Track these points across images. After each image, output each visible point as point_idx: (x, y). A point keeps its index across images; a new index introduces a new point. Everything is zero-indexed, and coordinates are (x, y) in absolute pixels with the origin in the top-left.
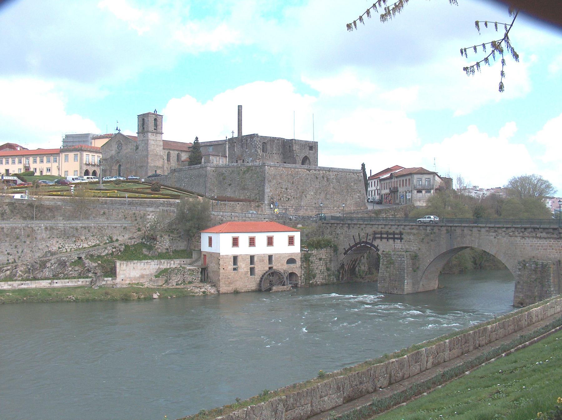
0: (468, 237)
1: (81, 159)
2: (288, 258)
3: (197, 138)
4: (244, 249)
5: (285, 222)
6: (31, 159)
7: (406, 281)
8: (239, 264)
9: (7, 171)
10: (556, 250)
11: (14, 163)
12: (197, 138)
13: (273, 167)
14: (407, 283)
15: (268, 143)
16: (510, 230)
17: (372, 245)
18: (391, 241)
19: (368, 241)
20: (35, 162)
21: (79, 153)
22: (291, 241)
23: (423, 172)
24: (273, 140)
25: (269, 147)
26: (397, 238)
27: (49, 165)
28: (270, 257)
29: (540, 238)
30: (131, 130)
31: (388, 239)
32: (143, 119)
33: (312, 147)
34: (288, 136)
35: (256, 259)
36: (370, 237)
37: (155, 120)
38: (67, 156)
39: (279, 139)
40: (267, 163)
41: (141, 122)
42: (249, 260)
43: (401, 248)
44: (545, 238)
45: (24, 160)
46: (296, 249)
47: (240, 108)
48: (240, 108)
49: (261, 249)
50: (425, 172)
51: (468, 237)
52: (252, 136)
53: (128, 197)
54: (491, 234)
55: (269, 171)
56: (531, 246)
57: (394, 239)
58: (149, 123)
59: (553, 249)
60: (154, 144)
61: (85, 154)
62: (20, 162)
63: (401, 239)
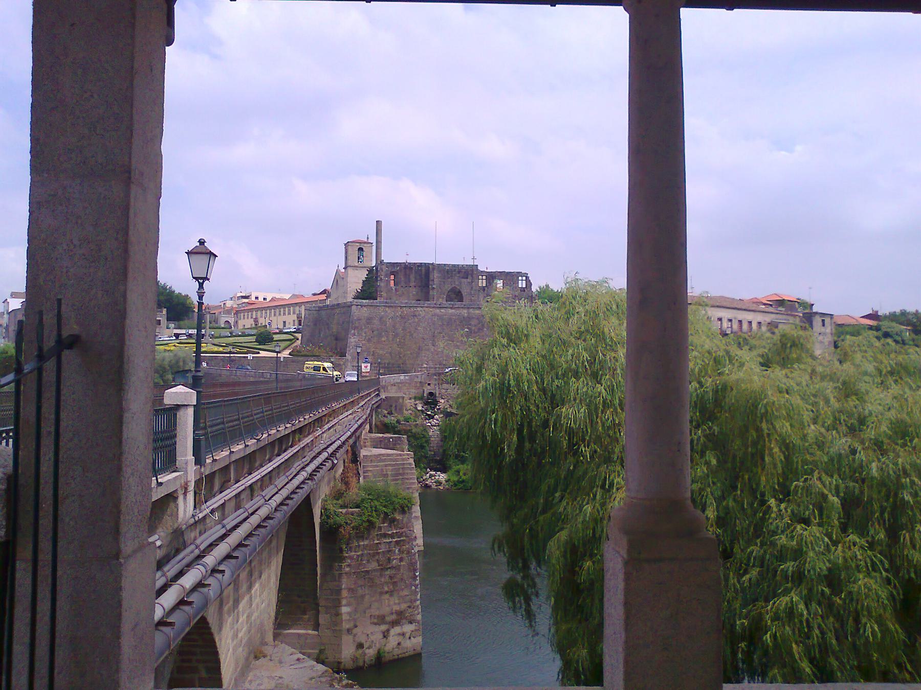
24: (407, 268)
37: (361, 249)
45: (297, 308)
62: (294, 313)
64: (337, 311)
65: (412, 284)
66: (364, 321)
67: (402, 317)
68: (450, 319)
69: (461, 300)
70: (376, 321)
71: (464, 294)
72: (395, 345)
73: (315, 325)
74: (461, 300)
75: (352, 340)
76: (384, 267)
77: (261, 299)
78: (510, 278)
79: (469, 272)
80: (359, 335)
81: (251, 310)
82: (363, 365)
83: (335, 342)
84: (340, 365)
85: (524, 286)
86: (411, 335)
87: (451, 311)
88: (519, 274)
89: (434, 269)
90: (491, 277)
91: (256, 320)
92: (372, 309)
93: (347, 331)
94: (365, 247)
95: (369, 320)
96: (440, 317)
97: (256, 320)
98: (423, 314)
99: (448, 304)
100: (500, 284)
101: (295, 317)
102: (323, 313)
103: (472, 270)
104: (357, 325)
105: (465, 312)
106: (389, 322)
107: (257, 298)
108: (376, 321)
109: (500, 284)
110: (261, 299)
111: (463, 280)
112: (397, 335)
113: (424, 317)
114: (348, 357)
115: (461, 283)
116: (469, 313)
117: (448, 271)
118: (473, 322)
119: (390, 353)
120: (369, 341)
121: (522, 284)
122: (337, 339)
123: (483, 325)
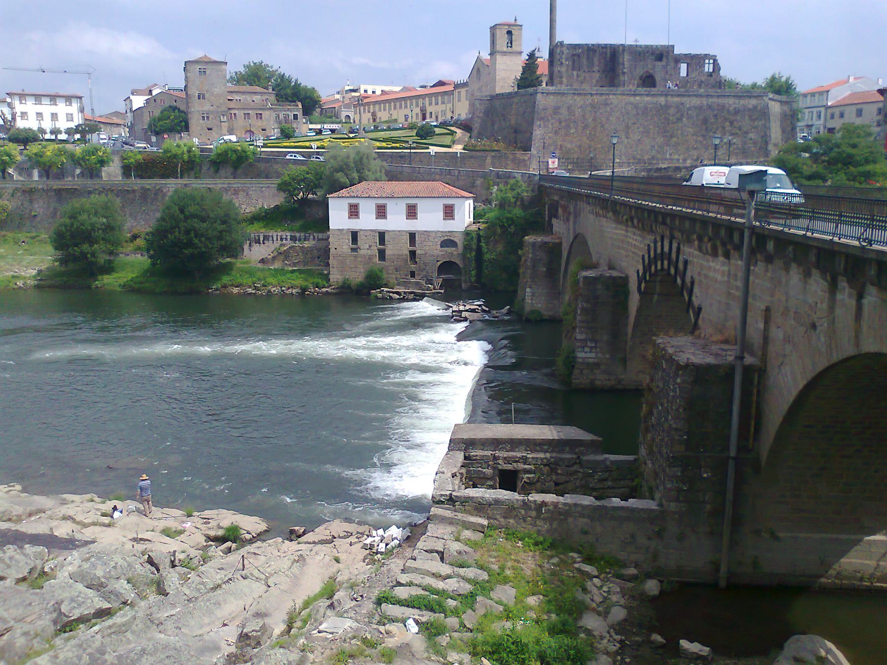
2: (442, 239)
4: (367, 221)
7: (528, 290)
14: (533, 294)
22: (449, 212)
24: (590, 50)
27: (443, 107)
28: (412, 236)
35: (360, 237)
37: (509, 33)
39: (605, 46)
45: (420, 101)
49: (396, 221)
53: (318, 148)
64: (516, 100)
65: (596, 69)
66: (550, 111)
67: (593, 106)
68: (646, 108)
69: (653, 85)
70: (564, 111)
71: (658, 78)
72: (585, 138)
73: (487, 116)
74: (653, 85)
75: (538, 133)
76: (564, 49)
77: (370, 92)
78: (695, 61)
79: (662, 54)
80: (545, 126)
81: (368, 104)
82: (550, 161)
83: (513, 135)
84: (524, 160)
85: (711, 70)
86: (602, 126)
88: (706, 56)
89: (624, 51)
90: (678, 59)
91: (374, 114)
92: (559, 97)
93: (531, 123)
94: (512, 29)
95: (556, 110)
96: (636, 106)
97: (374, 114)
99: (642, 90)
100: (683, 67)
101: (418, 110)
102: (497, 103)
103: (668, 52)
104: (543, 115)
105: (662, 100)
106: (578, 112)
107: (366, 91)
108: (564, 111)
109: (683, 67)
110: (370, 92)
111: (659, 63)
112: (586, 127)
113: (616, 106)
114: (534, 151)
115: (654, 66)
116: (666, 101)
117: (640, 54)
118: (672, 111)
119: (580, 147)
120: (556, 133)
121: (708, 68)
123: (682, 115)
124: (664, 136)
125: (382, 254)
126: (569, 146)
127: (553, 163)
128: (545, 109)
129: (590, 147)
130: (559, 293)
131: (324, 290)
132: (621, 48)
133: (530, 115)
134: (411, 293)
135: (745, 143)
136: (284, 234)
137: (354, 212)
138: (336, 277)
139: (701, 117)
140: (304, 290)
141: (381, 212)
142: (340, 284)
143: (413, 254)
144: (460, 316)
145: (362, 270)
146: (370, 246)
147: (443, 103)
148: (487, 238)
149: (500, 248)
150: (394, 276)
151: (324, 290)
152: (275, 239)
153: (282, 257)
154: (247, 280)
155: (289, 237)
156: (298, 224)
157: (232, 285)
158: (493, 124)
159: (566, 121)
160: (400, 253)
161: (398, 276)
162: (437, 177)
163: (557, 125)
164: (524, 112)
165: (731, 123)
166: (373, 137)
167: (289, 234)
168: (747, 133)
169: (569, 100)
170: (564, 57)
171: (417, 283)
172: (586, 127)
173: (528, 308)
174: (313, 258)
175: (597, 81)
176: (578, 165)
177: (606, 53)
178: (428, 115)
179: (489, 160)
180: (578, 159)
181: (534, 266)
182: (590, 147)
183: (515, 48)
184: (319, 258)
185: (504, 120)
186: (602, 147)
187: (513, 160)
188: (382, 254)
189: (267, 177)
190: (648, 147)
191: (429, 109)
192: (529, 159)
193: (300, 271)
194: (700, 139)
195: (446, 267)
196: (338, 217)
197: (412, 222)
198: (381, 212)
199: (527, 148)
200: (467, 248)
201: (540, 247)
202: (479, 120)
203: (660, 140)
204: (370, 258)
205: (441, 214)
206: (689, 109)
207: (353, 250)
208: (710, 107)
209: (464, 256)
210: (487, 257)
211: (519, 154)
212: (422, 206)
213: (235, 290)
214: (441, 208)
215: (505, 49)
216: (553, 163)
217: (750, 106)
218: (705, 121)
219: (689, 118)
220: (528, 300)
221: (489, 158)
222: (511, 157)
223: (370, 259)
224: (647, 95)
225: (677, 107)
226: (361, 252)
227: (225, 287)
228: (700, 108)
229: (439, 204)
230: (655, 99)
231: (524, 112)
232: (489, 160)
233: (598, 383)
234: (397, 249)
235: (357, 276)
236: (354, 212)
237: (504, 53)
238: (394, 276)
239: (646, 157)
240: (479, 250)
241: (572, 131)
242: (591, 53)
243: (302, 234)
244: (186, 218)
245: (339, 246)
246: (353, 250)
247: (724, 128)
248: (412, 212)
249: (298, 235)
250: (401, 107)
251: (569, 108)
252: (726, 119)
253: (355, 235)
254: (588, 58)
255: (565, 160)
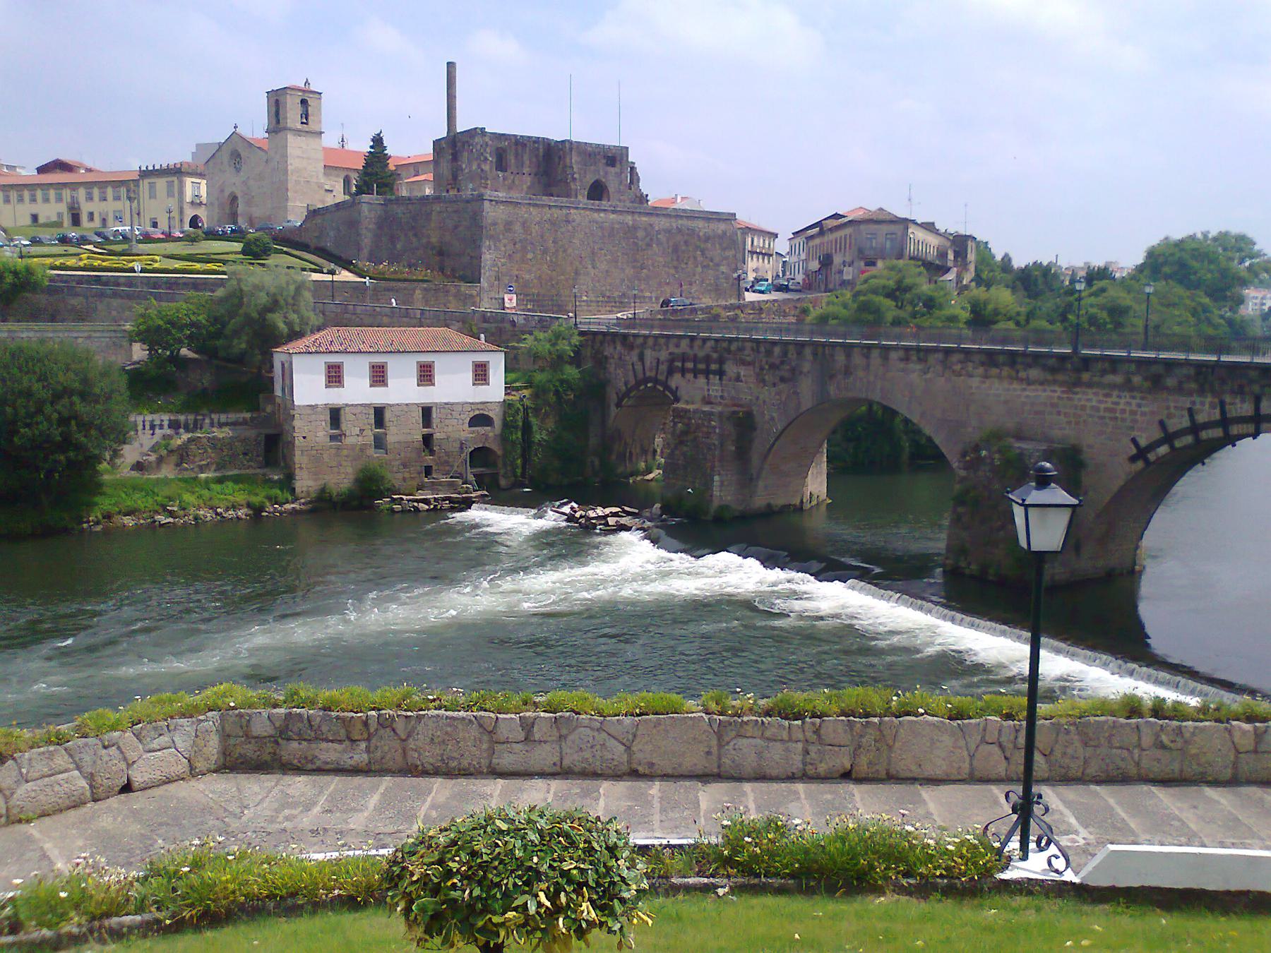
0: (860, 374)
1: (181, 192)
2: (472, 414)
3: (378, 141)
4: (357, 390)
5: (498, 331)
6: (82, 193)
7: (716, 478)
8: (344, 427)
9: (35, 218)
10: (1066, 415)
11: (46, 200)
12: (378, 141)
13: (503, 202)
14: (722, 482)
15: (510, 152)
16: (955, 358)
17: (667, 387)
18: (702, 380)
19: (648, 374)
20: (90, 198)
21: (175, 179)
22: (481, 374)
23: (881, 217)
24: (520, 143)
25: (511, 159)
26: (715, 373)
27: (118, 205)
28: (427, 411)
29: (1029, 382)
30: (255, 126)
31: (696, 372)
32: (276, 100)
33: (615, 157)
34: (556, 136)
36: (663, 368)
37: (304, 102)
38: (152, 186)
39: (537, 140)
40: (488, 193)
41: (274, 109)
42: (418, 415)
43: (722, 397)
44: (1042, 384)
45: (67, 194)
46: (495, 391)
47: (451, 66)
48: (451, 66)
49: (403, 389)
50: (888, 218)
51: (860, 374)
52: (472, 133)
54: (911, 366)
55: (492, 213)
56: (1006, 402)
57: (707, 373)
58: (291, 108)
59: (1059, 413)
60: (302, 156)
61: (189, 181)
62: (59, 199)
63: (721, 373)
65: (526, 170)
66: (501, 227)
70: (517, 227)
75: (488, 257)
80: (497, 249)
82: (507, 297)
83: (438, 258)
84: (471, 296)
86: (565, 251)
87: (612, 216)
92: (510, 208)
93: (474, 243)
95: (508, 225)
98: (578, 218)
101: (63, 208)
104: (492, 232)
106: (535, 229)
112: (545, 252)
115: (606, 173)
116: (634, 220)
118: (640, 234)
122: (441, 253)
124: (634, 267)
125: (379, 443)
126: (527, 277)
127: (511, 301)
128: (495, 224)
129: (551, 279)
130: (751, 479)
131: (288, 506)
132: (567, 145)
133: (474, 231)
134: (444, 499)
135: (717, 278)
136: (157, 418)
137: (335, 376)
138: (305, 483)
139: (671, 244)
140: (257, 510)
141: (379, 376)
142: (314, 495)
143: (427, 440)
144: (607, 524)
145: (350, 470)
146: (362, 430)
147: (117, 198)
148: (536, 411)
149: (550, 424)
150: (400, 476)
151: (288, 506)
152: (140, 427)
153: (174, 458)
154: (139, 500)
155: (166, 423)
156: (179, 399)
157: (119, 513)
158: (393, 239)
159: (521, 241)
160: (409, 438)
161: (407, 475)
162: (386, 320)
163: (510, 247)
164: (456, 227)
165: (703, 252)
166: (168, 252)
167: (166, 418)
168: (718, 265)
169: (523, 212)
170: (488, 150)
171: (451, 485)
172: (545, 252)
173: (716, 503)
174: (234, 456)
175: (529, 188)
176: (539, 303)
177: (538, 149)
178: (84, 218)
179: (418, 294)
180: (538, 295)
181: (722, 445)
182: (551, 279)
183: (312, 126)
184: (245, 454)
185: (415, 235)
186: (567, 280)
187: (456, 296)
188: (379, 443)
189: (53, 319)
190: (618, 281)
191: (86, 208)
192: (479, 294)
193: (237, 480)
194: (672, 271)
195: (480, 456)
196: (307, 386)
197: (379, 390)
198: (379, 376)
199: (475, 279)
200: (506, 425)
201: (728, 419)
202: (369, 235)
203: (629, 271)
204: (363, 448)
205: (469, 376)
206: (658, 232)
207: (333, 438)
208: (679, 230)
209: (503, 438)
210: (537, 437)
211: (464, 287)
212: (441, 364)
213: (129, 521)
214: (323, 368)
215: (299, 126)
216: (511, 301)
217: (720, 232)
218: (676, 249)
219: (659, 243)
220: (716, 493)
221: (418, 292)
222: (453, 290)
223: (361, 450)
224: (613, 212)
225: (645, 229)
226: (349, 441)
227: (108, 516)
228: (668, 231)
229: (467, 361)
230: (621, 218)
231: (456, 227)
232: (418, 294)
233: (1057, 578)
234: (404, 433)
235: (341, 480)
236: (335, 376)
237: (298, 132)
238: (400, 476)
239: (616, 294)
240: (527, 428)
241: (530, 256)
242: (520, 148)
243: (191, 417)
244: (57, 397)
245: (308, 435)
246: (333, 438)
247: (695, 258)
248: (426, 375)
249: (182, 418)
250: (21, 200)
251: (524, 224)
252: (697, 248)
253: (335, 415)
254: (516, 155)
255: (523, 296)
